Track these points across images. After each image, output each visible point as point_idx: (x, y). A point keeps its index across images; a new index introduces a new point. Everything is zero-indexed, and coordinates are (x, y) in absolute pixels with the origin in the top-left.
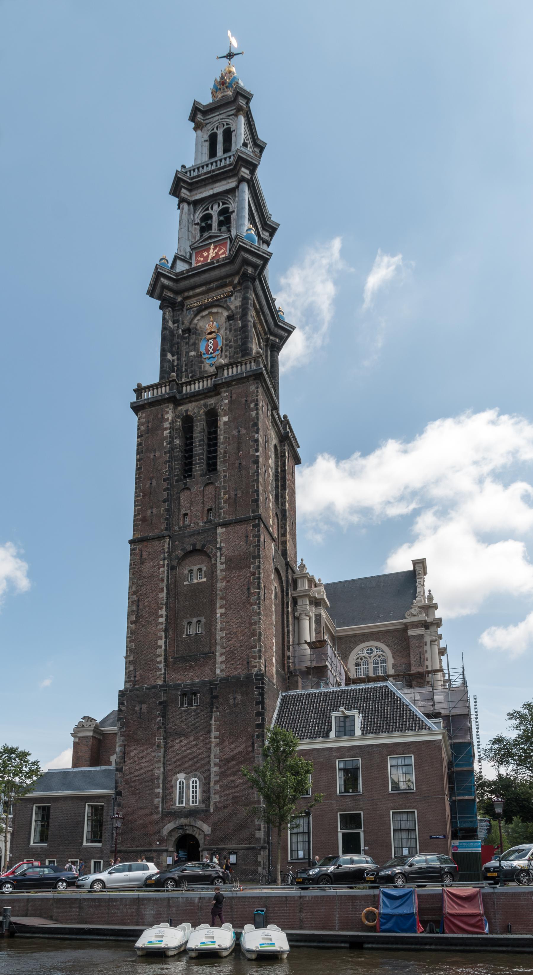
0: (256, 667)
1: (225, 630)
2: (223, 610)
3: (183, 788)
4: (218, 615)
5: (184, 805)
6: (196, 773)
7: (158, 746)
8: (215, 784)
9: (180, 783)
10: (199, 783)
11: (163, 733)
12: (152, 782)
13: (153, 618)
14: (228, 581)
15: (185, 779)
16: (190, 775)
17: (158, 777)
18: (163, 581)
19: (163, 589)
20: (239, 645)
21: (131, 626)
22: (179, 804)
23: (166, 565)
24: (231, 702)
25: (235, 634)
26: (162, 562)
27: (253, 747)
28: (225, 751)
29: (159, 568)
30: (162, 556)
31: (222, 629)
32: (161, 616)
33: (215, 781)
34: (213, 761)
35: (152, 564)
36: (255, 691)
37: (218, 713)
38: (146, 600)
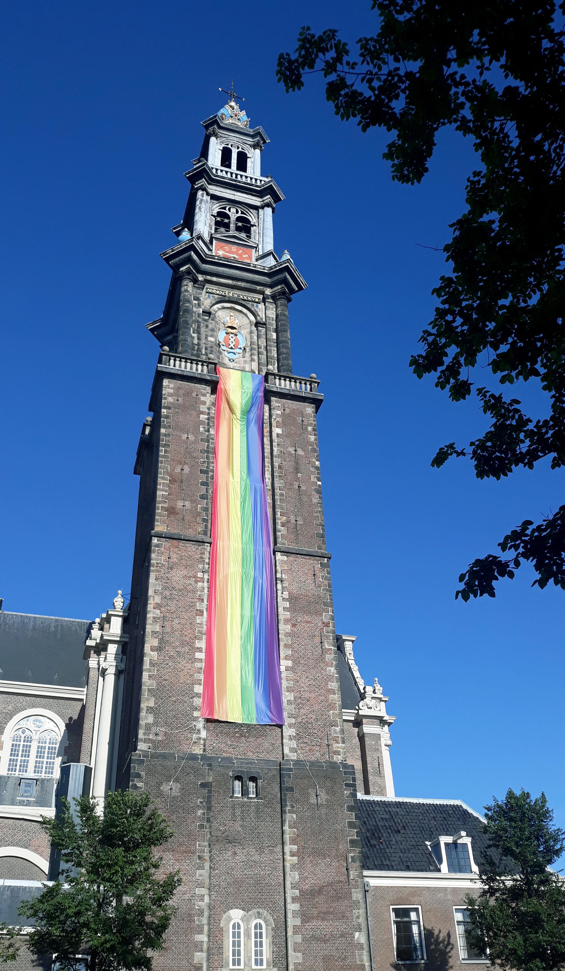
0: (339, 755)
1: (293, 691)
2: (290, 663)
3: (239, 937)
4: (282, 668)
5: (242, 967)
6: (261, 911)
7: (200, 858)
8: (295, 933)
9: (234, 927)
10: (266, 929)
11: (209, 836)
12: (189, 921)
13: (186, 649)
14: (294, 625)
15: (242, 919)
16: (250, 913)
17: (201, 912)
18: (202, 600)
19: (202, 612)
20: (314, 717)
21: (152, 653)
22: (234, 964)
23: (206, 580)
24: (313, 800)
25: (308, 701)
26: (200, 575)
27: (348, 876)
28: (307, 878)
29: (196, 582)
30: (201, 566)
31: (289, 690)
32: (200, 650)
33: (295, 927)
34: (290, 893)
35: (185, 572)
36: (345, 790)
37: (295, 816)
38: (177, 621)
